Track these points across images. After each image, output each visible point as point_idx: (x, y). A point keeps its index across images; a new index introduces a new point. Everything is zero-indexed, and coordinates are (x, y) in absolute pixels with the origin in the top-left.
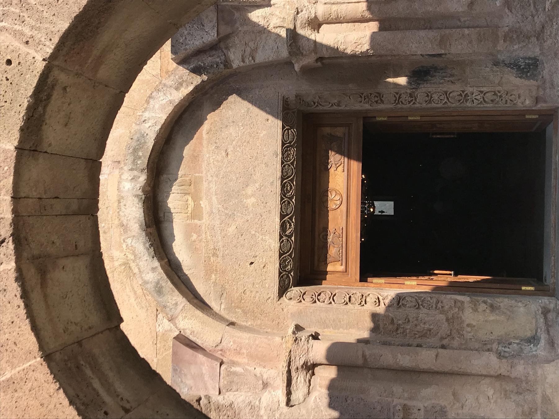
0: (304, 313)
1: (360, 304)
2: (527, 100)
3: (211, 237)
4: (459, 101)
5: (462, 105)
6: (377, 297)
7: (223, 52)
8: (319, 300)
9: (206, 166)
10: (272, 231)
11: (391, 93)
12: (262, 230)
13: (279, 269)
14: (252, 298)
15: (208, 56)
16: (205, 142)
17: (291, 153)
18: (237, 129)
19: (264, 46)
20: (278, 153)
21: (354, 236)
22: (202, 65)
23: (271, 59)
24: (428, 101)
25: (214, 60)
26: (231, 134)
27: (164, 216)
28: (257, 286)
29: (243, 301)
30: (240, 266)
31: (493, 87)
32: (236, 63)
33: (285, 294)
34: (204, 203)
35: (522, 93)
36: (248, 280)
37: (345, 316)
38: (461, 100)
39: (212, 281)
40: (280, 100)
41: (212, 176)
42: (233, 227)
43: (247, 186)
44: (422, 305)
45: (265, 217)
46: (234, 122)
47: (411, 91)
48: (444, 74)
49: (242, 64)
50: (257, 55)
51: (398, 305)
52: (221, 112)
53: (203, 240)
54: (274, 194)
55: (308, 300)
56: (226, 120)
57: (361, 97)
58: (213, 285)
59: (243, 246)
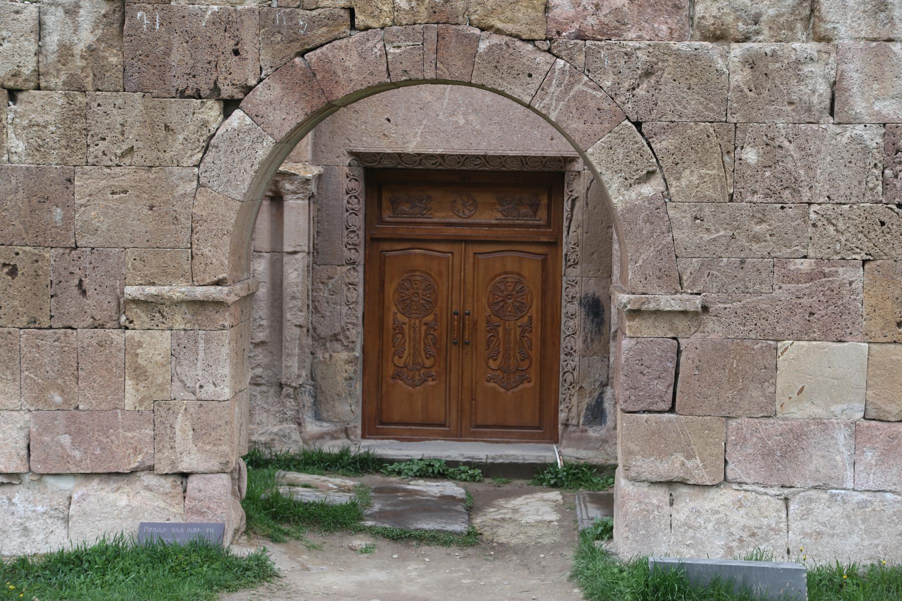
4: (566, 347)
8: (350, 197)
36: (369, 116)
42: (429, 98)
44: (350, 308)
48: (594, 333)
59: (408, 109)
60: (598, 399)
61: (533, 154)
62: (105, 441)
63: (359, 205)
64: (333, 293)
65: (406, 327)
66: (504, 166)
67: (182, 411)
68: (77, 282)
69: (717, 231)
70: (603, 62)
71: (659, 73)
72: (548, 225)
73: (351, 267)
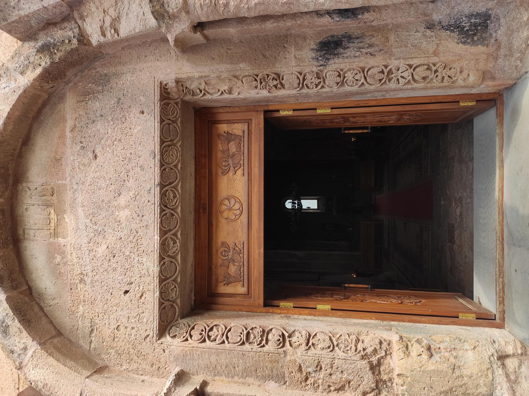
0: (189, 356)
1: (260, 344)
2: (471, 75)
3: (78, 259)
4: (380, 80)
5: (384, 86)
6: (281, 334)
7: (77, 23)
9: (70, 171)
10: (149, 251)
11: (292, 74)
12: (139, 250)
13: (159, 298)
14: (127, 336)
15: (59, 29)
16: (68, 141)
17: (174, 153)
18: (106, 124)
19: (127, 14)
20: (156, 153)
21: (257, 252)
22: (52, 41)
23: (137, 30)
24: (340, 83)
25: (66, 34)
26: (98, 131)
29: (116, 340)
30: (112, 296)
31: (426, 59)
32: (95, 38)
33: (167, 331)
35: (464, 65)
36: (121, 313)
37: (241, 361)
38: (383, 78)
39: (79, 313)
40: (156, 87)
41: (77, 183)
42: (104, 247)
43: (119, 195)
44: (337, 345)
45: (142, 234)
46: (102, 116)
47: (318, 68)
48: (360, 45)
49: (102, 39)
50: (121, 26)
51: (307, 345)
52: (86, 103)
53: (69, 263)
54: (152, 204)
55: (196, 339)
56: (92, 113)
57: (256, 80)
58: (81, 319)
59: (115, 270)
61: (157, 133)
66: (176, 166)
73: (287, 340)
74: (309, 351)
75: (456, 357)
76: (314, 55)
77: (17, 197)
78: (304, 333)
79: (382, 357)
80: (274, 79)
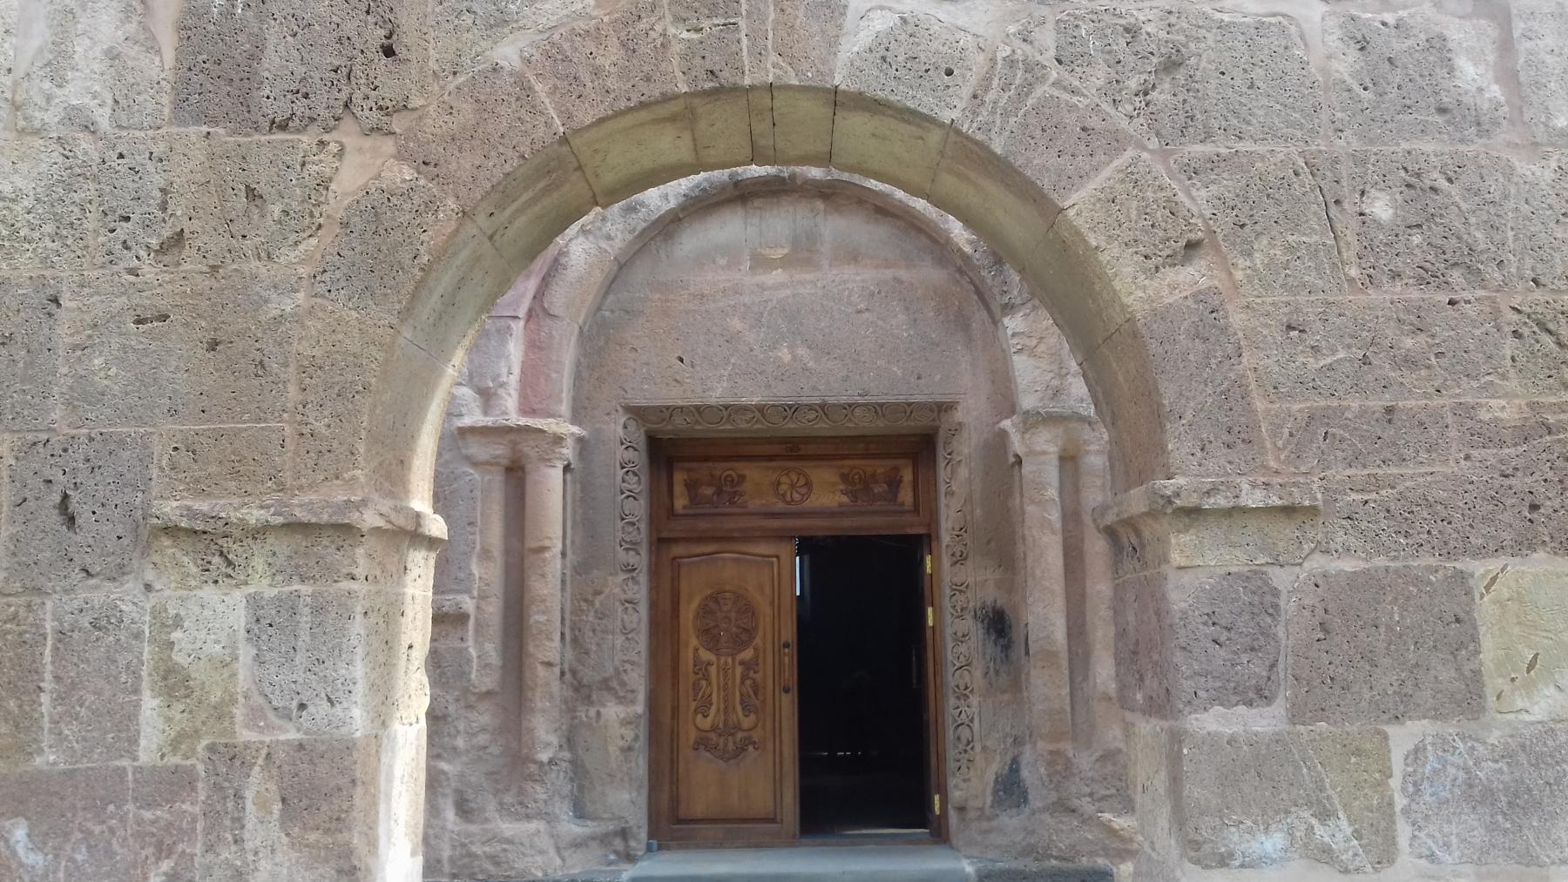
4: (958, 687)
27: (755, 208)
28: (644, 370)
29: (618, 348)
32: (1013, 323)
34: (778, 276)
43: (809, 347)
46: (915, 320)
48: (998, 660)
49: (1010, 332)
50: (1025, 358)
59: (709, 343)
60: (1012, 764)
61: (891, 399)
62: (97, 829)
63: (638, 484)
64: (601, 615)
65: (713, 670)
66: (850, 420)
67: (260, 761)
68: (57, 498)
69: (1334, 351)
70: (1084, 43)
71: (1193, 60)
72: (916, 509)
74: (617, 603)
75: (622, 780)
76: (989, 603)
77: (804, 197)
78: (638, 596)
79: (617, 692)
80: (962, 552)
